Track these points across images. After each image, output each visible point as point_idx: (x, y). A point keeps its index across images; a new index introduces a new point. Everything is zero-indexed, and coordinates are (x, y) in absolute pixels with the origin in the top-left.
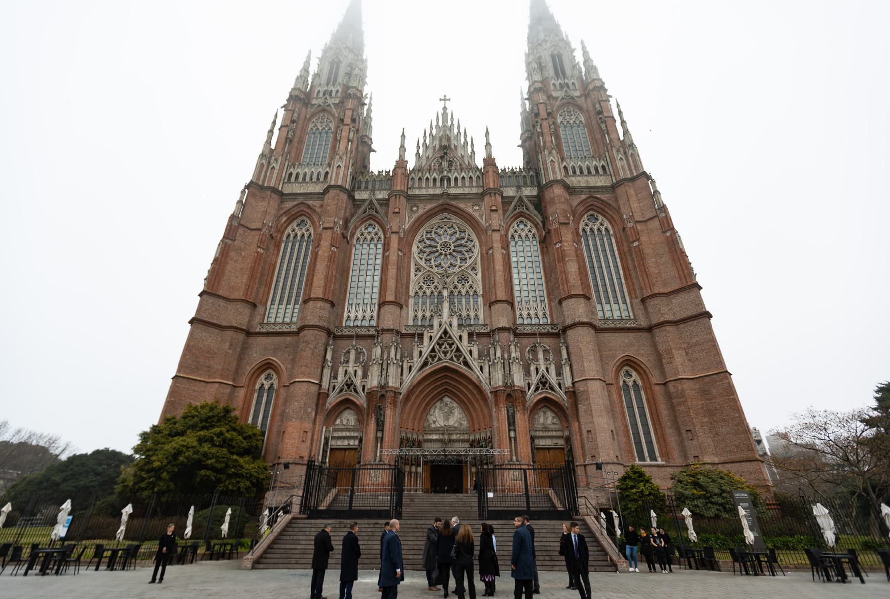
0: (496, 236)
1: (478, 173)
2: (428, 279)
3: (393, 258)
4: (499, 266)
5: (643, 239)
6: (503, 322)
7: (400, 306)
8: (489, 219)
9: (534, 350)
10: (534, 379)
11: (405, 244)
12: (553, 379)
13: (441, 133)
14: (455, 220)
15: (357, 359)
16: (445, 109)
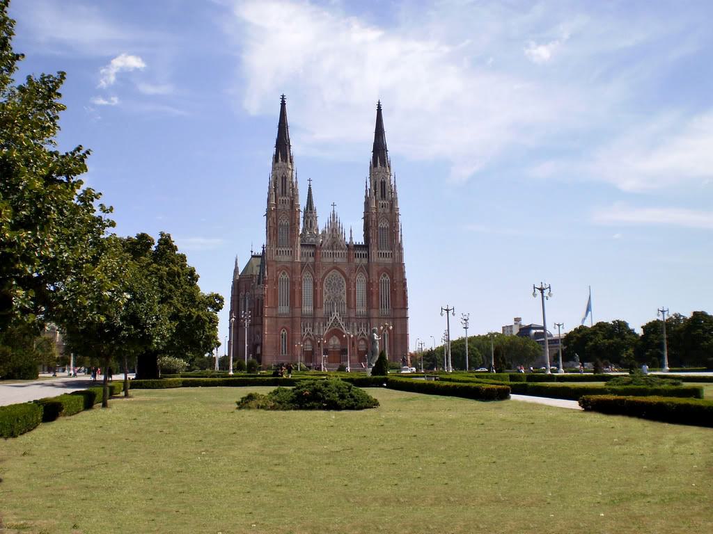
0: (352, 284)
1: (347, 251)
2: (329, 298)
3: (319, 291)
4: (352, 296)
5: (398, 289)
6: (353, 315)
7: (321, 307)
8: (350, 275)
9: (361, 324)
10: (360, 333)
11: (321, 284)
12: (365, 333)
13: (332, 227)
14: (339, 274)
15: (310, 326)
16: (334, 211)
